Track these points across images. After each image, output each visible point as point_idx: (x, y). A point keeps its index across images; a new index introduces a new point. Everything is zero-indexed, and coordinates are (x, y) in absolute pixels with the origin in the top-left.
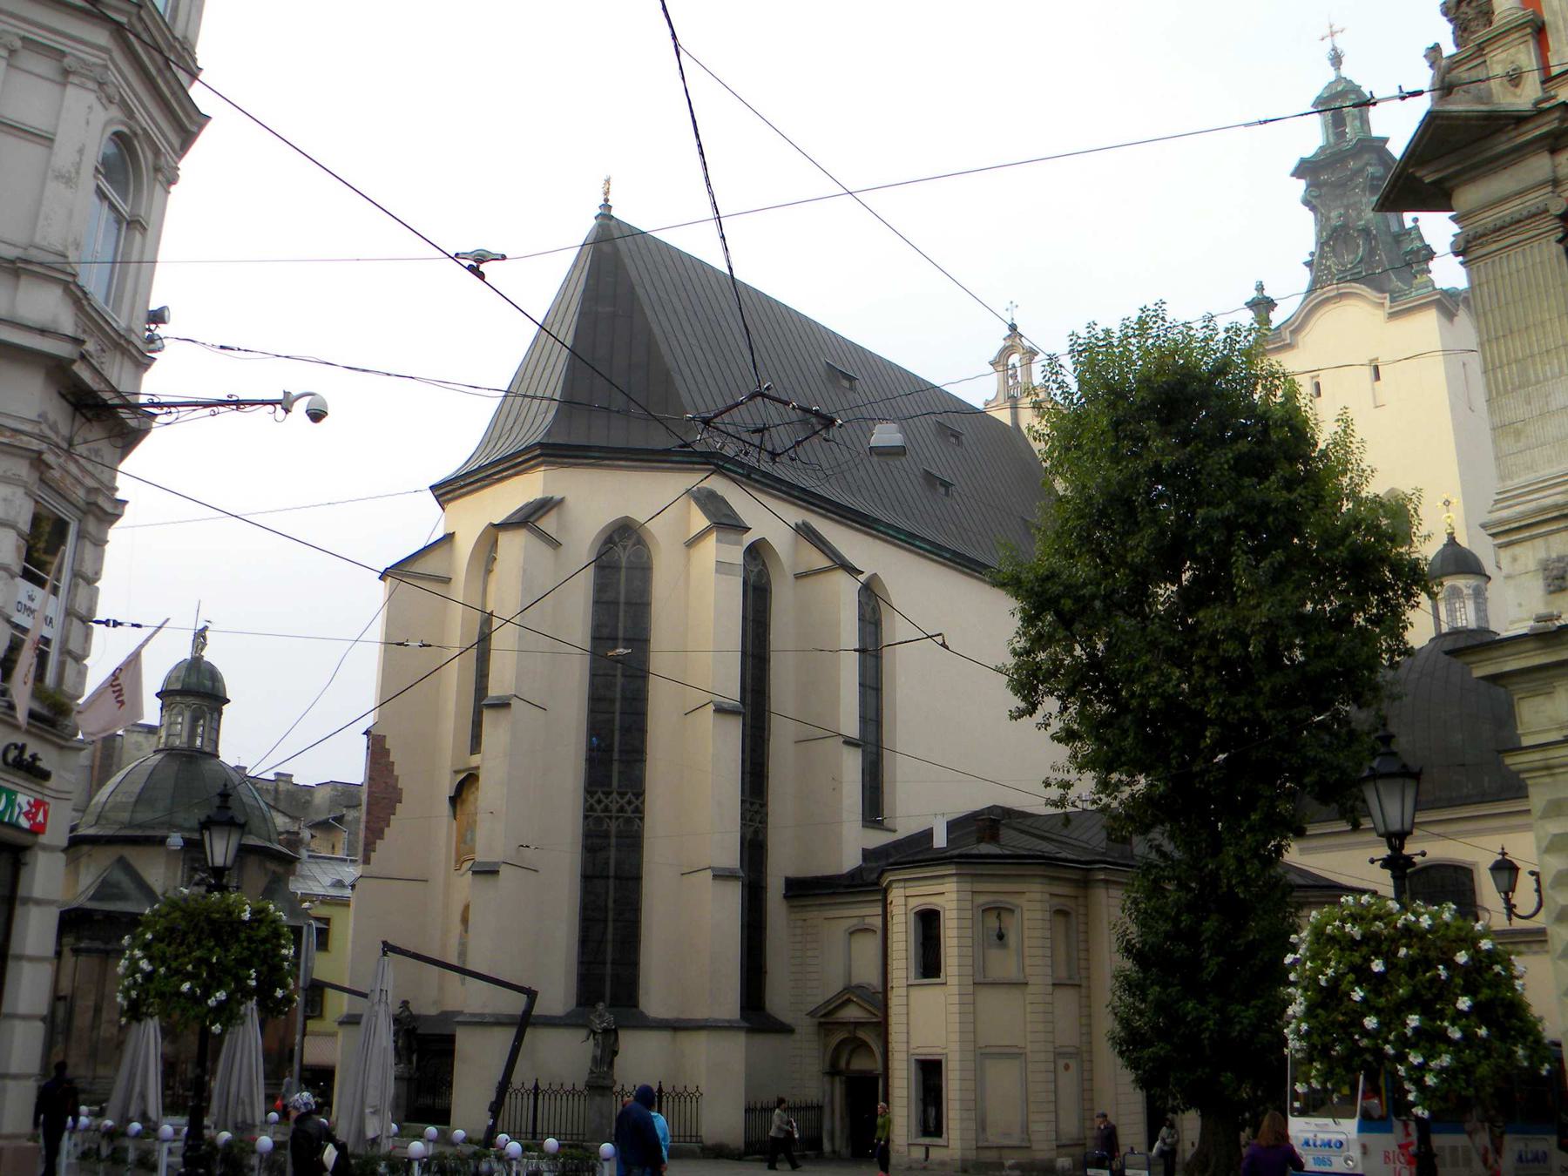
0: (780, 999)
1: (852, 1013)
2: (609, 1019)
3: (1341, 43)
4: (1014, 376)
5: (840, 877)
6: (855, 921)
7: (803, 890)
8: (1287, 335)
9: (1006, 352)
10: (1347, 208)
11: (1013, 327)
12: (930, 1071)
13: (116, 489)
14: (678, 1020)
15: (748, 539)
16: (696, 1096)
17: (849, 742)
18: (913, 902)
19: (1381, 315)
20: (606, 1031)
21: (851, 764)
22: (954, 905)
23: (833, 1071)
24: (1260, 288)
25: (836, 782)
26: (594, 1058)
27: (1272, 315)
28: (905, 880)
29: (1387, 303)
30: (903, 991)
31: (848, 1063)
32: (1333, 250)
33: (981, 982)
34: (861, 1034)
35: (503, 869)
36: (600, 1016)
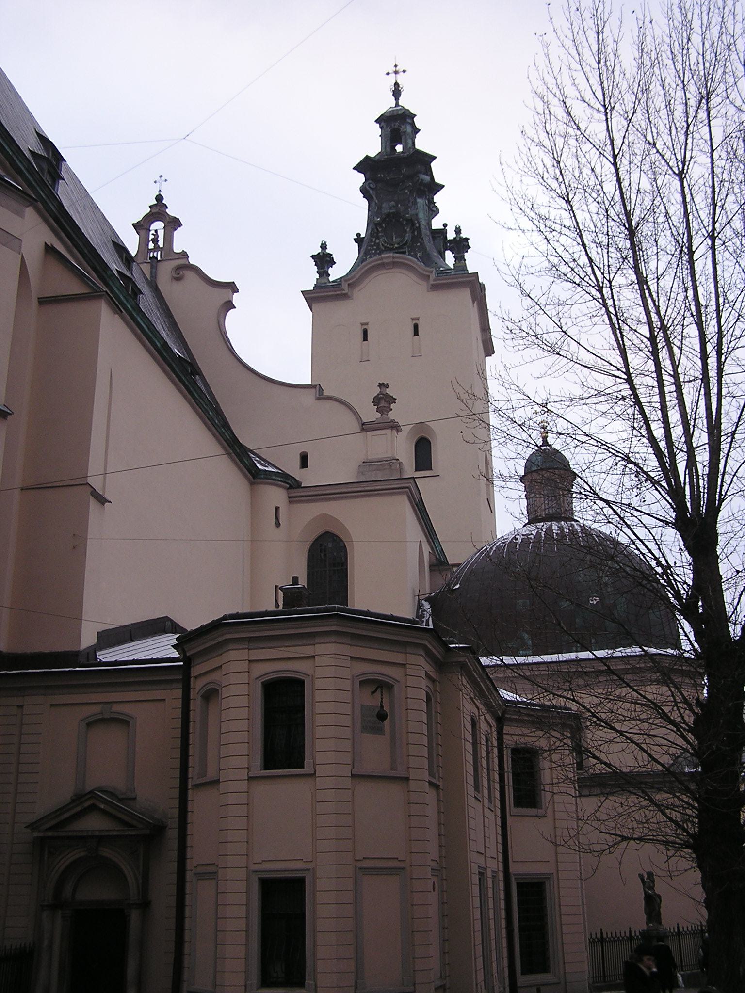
1: (94, 824)
3: (401, 79)
4: (155, 241)
5: (77, 654)
6: (96, 709)
8: (345, 286)
9: (151, 218)
10: (397, 203)
11: (159, 198)
18: (261, 669)
19: (423, 285)
24: (324, 246)
27: (330, 271)
28: (250, 639)
29: (433, 276)
30: (243, 786)
34: (106, 852)
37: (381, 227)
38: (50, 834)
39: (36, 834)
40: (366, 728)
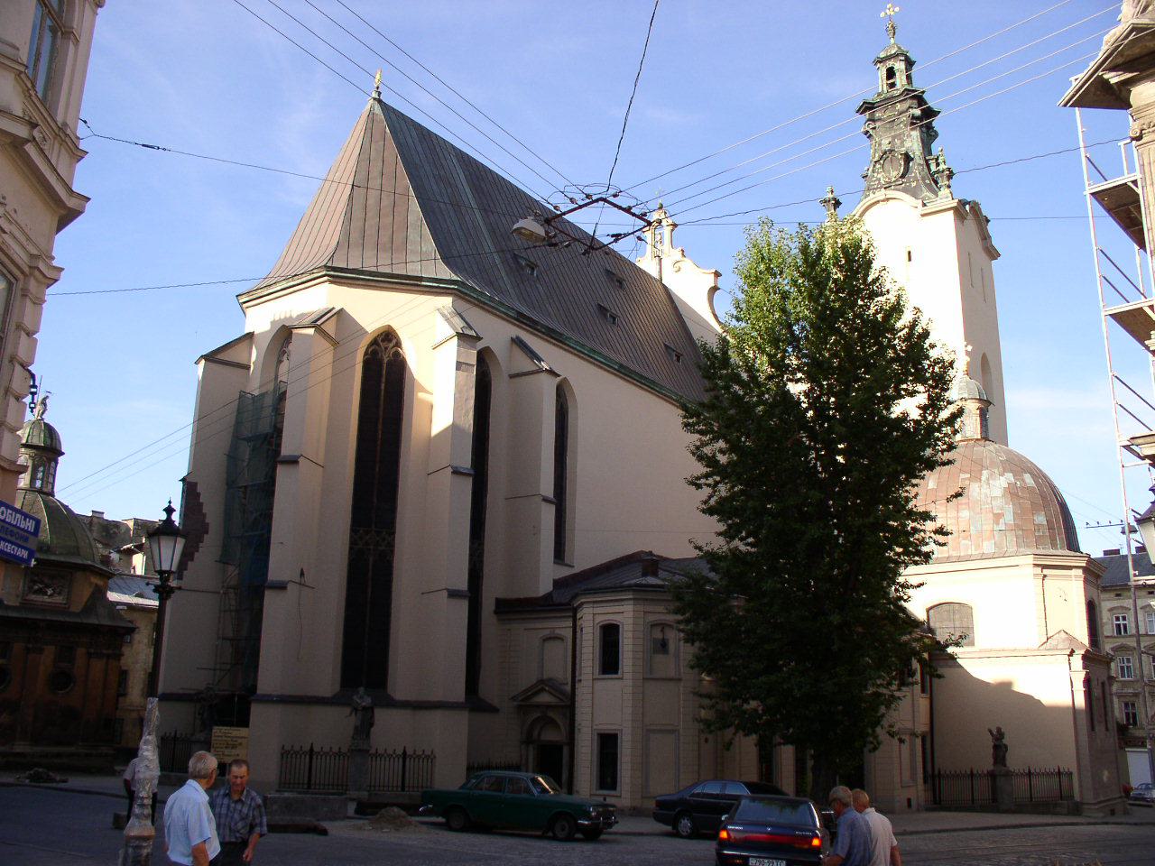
0: (490, 688)
1: (544, 698)
2: (367, 701)
7: (511, 608)
12: (608, 742)
13: (53, 258)
14: (415, 702)
15: (480, 345)
16: (430, 758)
17: (546, 500)
20: (364, 708)
21: (548, 513)
22: (631, 621)
23: (528, 740)
25: (536, 531)
26: (356, 728)
28: (594, 602)
31: (539, 735)
33: (649, 676)
34: (551, 714)
35: (289, 587)
36: (361, 698)
38: (523, 703)
39: (515, 703)
40: (655, 652)
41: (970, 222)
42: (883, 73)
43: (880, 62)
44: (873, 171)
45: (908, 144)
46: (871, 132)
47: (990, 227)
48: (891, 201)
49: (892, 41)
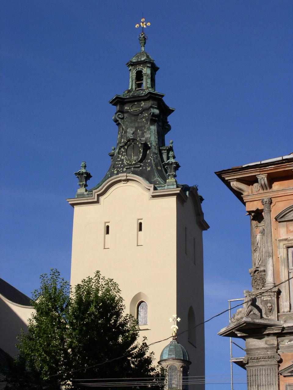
10: (137, 128)
32: (126, 151)
37: (124, 149)
41: (189, 204)
42: (133, 74)
43: (132, 65)
44: (119, 153)
45: (147, 135)
46: (120, 121)
47: (204, 205)
48: (130, 183)
49: (143, 49)
